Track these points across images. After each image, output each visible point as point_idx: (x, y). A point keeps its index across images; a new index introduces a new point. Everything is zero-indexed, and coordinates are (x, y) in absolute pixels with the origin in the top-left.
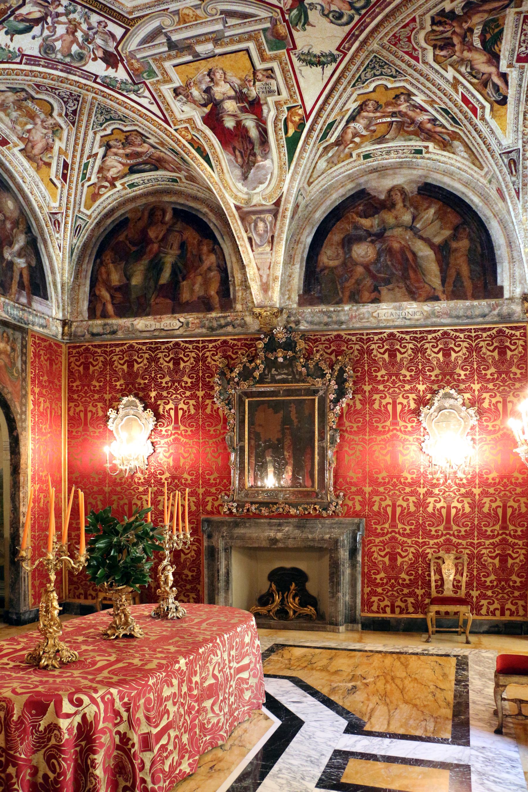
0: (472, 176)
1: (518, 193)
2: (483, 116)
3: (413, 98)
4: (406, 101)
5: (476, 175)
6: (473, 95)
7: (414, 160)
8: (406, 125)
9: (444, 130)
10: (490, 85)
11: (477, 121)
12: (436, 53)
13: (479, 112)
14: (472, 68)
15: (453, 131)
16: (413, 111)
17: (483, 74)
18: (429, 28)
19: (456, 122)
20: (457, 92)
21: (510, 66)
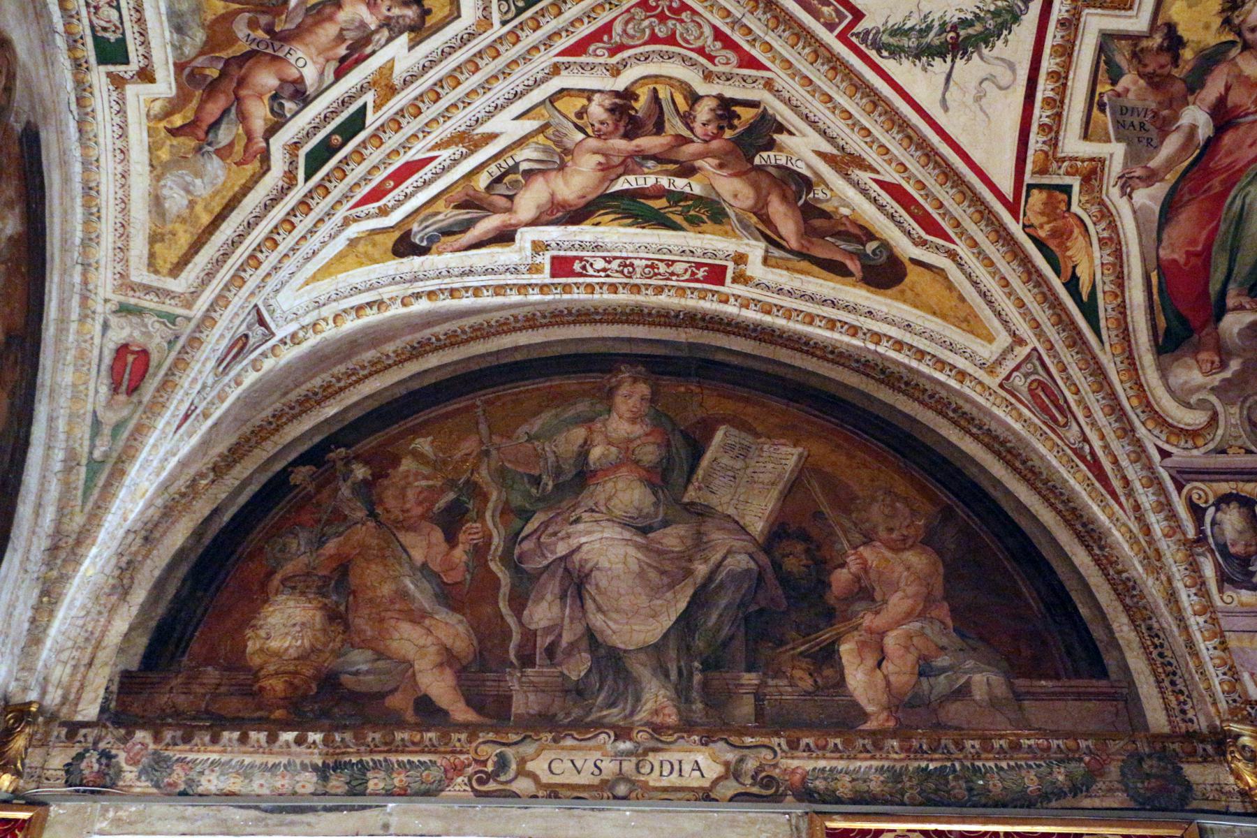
0: (90, 240)
1: (187, 417)
2: (358, 219)
3: (404, 38)
4: (387, 23)
5: (104, 251)
6: (426, 183)
7: (60, 41)
8: (264, 20)
9: (258, 125)
10: (464, 215)
11: (341, 212)
12: (597, 97)
13: (372, 207)
14: (529, 174)
15: (265, 157)
16: (340, 38)
17: (510, 198)
18: (701, 88)
19: (317, 159)
20: (437, 146)
21: (539, 247)
